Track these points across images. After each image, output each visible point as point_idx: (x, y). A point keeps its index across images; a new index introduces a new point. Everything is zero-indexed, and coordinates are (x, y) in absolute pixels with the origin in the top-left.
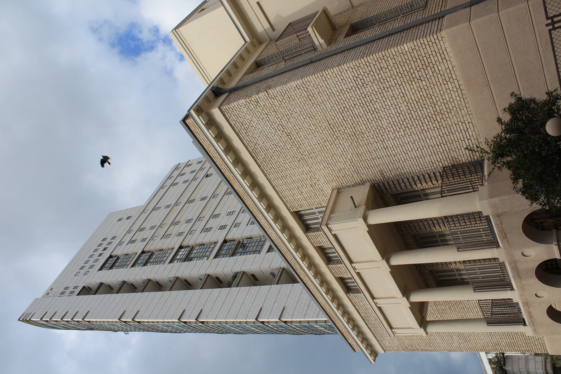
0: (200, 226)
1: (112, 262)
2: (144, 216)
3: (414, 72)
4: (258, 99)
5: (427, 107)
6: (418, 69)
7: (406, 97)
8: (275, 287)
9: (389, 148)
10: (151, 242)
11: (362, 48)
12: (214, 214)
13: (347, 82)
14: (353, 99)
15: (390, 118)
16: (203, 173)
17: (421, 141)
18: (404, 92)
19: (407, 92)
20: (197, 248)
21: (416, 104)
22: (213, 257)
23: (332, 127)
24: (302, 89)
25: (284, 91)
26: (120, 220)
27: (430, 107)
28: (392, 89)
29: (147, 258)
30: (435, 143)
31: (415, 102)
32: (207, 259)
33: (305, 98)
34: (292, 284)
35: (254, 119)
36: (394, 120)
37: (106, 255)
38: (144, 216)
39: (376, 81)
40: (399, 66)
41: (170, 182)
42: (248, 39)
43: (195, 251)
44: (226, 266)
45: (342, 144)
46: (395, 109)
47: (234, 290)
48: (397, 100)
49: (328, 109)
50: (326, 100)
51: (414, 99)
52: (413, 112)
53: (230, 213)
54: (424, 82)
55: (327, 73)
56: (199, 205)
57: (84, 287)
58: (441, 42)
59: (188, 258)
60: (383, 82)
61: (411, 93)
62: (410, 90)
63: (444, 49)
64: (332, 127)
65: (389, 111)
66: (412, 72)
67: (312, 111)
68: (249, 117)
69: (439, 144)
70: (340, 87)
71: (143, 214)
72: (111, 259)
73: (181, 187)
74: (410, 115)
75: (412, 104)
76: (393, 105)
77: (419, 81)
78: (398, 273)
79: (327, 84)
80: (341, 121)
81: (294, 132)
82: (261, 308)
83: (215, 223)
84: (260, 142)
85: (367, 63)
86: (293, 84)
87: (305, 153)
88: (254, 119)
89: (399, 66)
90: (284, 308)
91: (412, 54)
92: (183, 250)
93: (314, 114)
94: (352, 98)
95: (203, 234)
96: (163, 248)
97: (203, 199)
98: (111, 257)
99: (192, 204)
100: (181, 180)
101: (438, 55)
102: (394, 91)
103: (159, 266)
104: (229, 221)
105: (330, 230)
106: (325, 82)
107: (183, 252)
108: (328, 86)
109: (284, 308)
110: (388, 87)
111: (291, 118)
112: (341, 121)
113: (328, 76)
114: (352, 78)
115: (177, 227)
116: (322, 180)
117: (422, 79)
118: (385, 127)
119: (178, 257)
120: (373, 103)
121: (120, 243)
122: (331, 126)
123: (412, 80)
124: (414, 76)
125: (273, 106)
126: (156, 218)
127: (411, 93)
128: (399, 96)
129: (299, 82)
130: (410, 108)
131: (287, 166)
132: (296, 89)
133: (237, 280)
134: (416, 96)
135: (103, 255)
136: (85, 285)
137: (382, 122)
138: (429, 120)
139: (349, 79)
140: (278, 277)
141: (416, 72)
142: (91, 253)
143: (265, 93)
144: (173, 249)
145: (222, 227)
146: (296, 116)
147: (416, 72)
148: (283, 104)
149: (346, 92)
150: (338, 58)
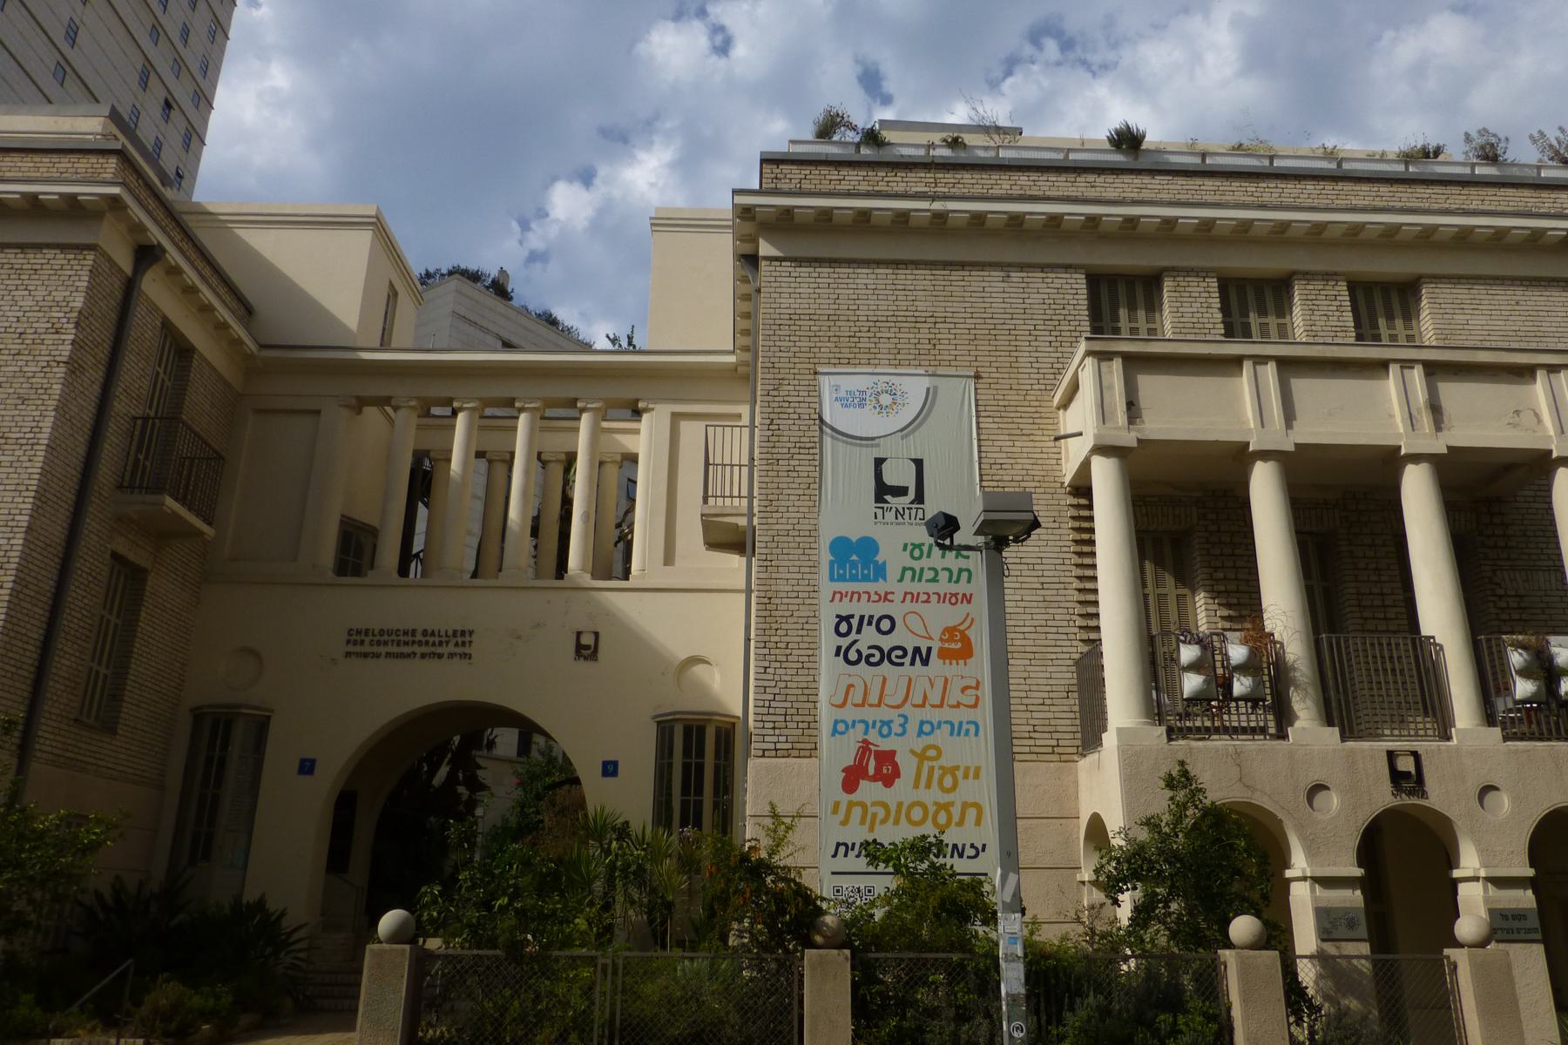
11: (49, 586)
68: (41, 292)
86: (47, 424)
129: (44, 438)
150: (56, 532)
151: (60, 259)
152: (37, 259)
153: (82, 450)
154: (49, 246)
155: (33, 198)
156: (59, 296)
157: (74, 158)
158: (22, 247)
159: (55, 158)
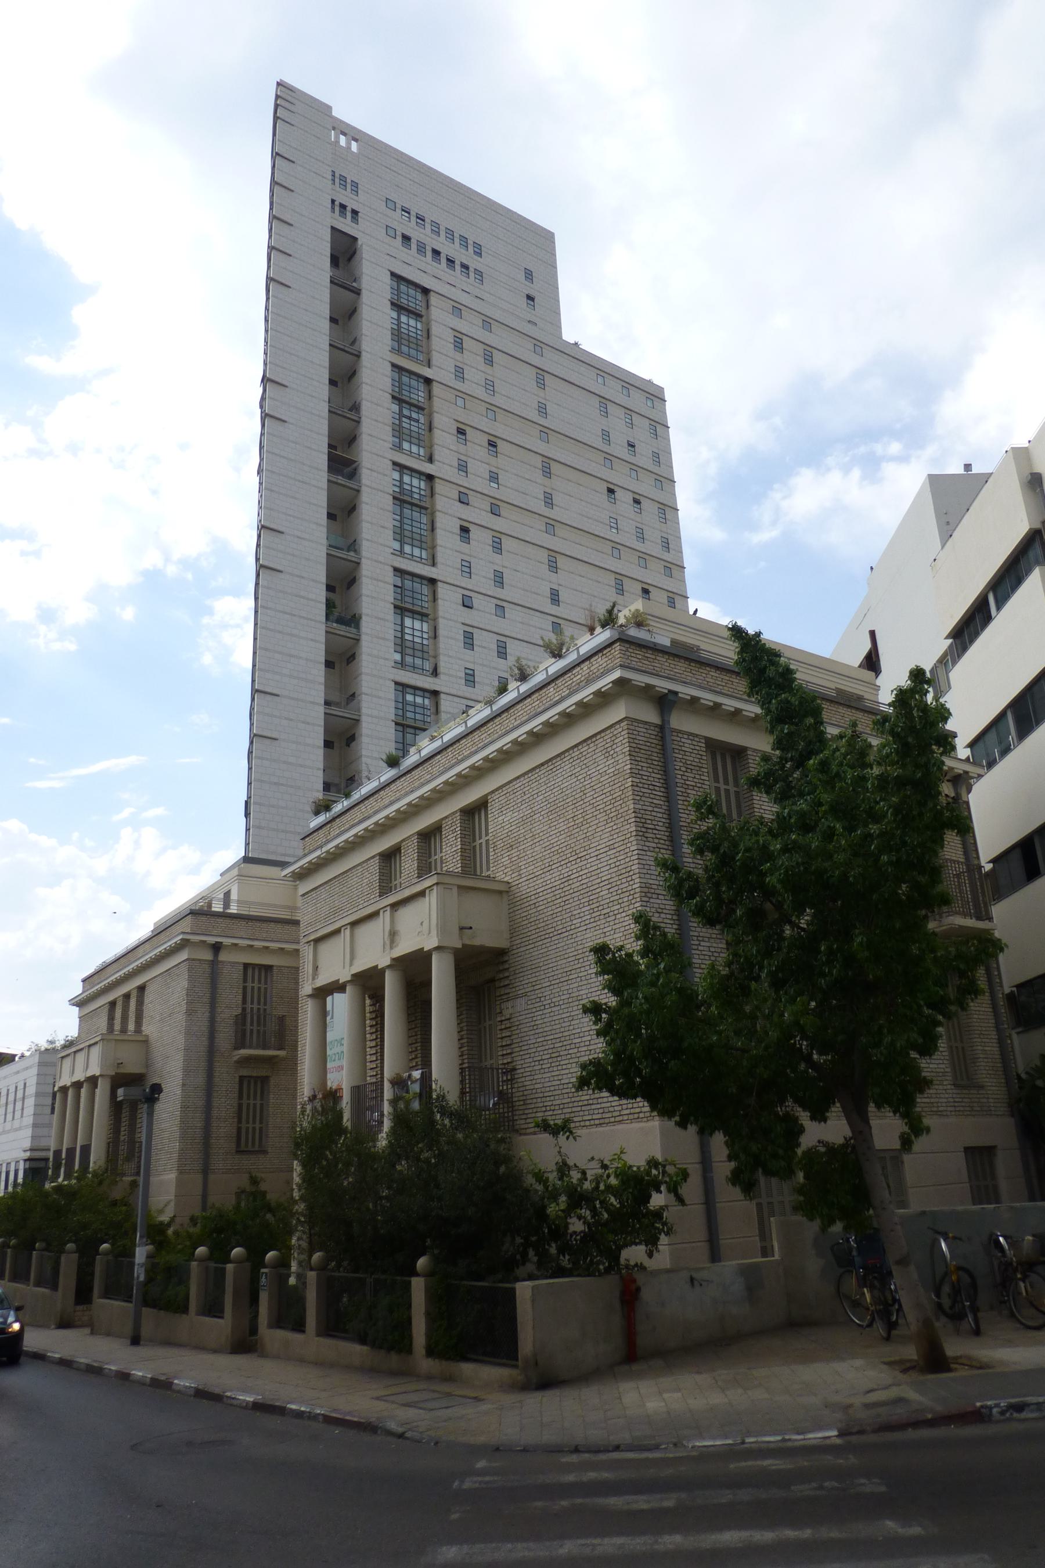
16: (618, 477)
22: (397, 565)
26: (529, 275)
29: (413, 395)
43: (416, 515)
44: (375, 597)
53: (499, 579)
57: (355, 239)
59: (401, 500)
92: (423, 485)
96: (437, 433)
98: (426, 291)
100: (616, 422)
119: (406, 479)
121: (458, 310)
126: (516, 391)
136: (360, 242)
140: (341, 714)
144: (431, 460)
150: (200, 1079)
153: (206, 1043)
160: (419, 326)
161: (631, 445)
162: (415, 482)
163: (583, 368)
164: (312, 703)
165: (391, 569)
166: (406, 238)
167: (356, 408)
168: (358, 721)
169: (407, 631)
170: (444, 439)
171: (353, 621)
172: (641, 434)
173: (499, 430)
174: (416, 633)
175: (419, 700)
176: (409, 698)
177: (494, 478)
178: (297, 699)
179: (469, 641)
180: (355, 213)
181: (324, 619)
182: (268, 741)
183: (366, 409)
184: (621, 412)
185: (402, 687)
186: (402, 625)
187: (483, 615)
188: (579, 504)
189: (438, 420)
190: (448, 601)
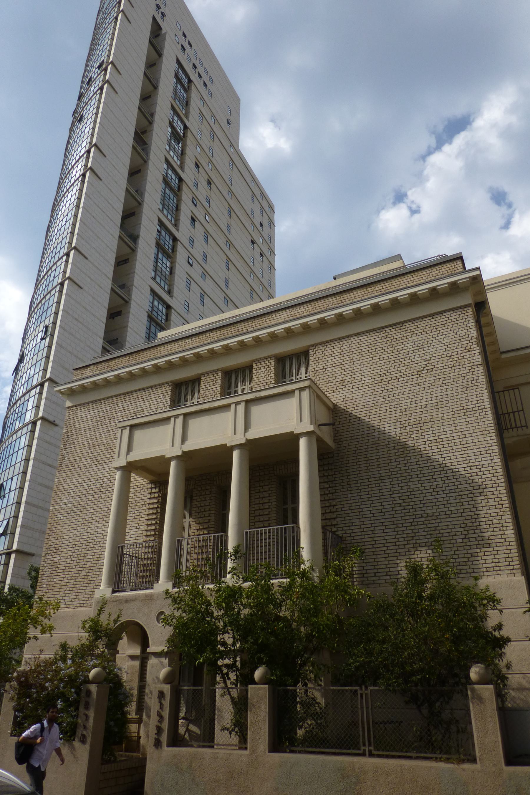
0: (199, 214)
1: (184, 82)
2: (226, 144)
3: (475, 533)
4: (473, 352)
5: (427, 537)
6: (478, 539)
7: (444, 517)
8: (108, 284)
9: (380, 482)
10: (195, 143)
12: (209, 237)
13: (477, 457)
14: (452, 458)
15: (420, 492)
17: (383, 521)
18: (451, 516)
19: (452, 519)
20: (175, 201)
21: (433, 525)
23: (420, 425)
24: (477, 405)
25: (478, 384)
27: (426, 540)
28: (458, 504)
30: (377, 535)
31: (436, 525)
32: (159, 209)
33: (464, 405)
34: (107, 306)
35: (447, 341)
36: (416, 496)
37: (194, 77)
38: (226, 144)
39: (471, 488)
40: (487, 519)
41: (257, 193)
42: (504, 356)
43: (172, 196)
45: (395, 430)
46: (430, 501)
47: (116, 231)
48: (443, 506)
49: (444, 427)
50: (457, 428)
51: (440, 524)
52: (423, 519)
54: (461, 541)
55: (492, 438)
56: (223, 221)
58: (509, 572)
60: (469, 496)
61: (449, 523)
62: (453, 523)
63: (499, 572)
64: (420, 425)
65: (430, 494)
66: (476, 531)
67: (445, 408)
68: (451, 334)
69: (375, 539)
70: (472, 448)
71: (229, 144)
72: (187, 80)
73: (248, 205)
74: (420, 516)
75: (433, 521)
76: (436, 500)
77: (463, 537)
78: (223, 453)
79: (478, 434)
80: (426, 436)
81: (420, 380)
82: (87, 258)
83: (198, 232)
84: (414, 338)
85: (496, 485)
87: (390, 385)
88: (447, 341)
89: (487, 519)
90: (81, 288)
91: (500, 536)
92: (177, 181)
93: (440, 409)
94: (454, 457)
95: (190, 215)
97: (229, 228)
98: (190, 81)
99: (226, 212)
101: (494, 565)
102: (455, 505)
103: (165, 142)
104: (197, 253)
105: (301, 389)
106: (482, 433)
107: (174, 180)
108: (475, 434)
109: (81, 288)
110: (462, 500)
111: (440, 383)
112: (426, 436)
113: (489, 438)
114: (481, 463)
115: (205, 183)
116: (349, 395)
117: (465, 540)
118: (409, 484)
119: (170, 172)
120: (443, 479)
122: (422, 425)
123: (466, 529)
124: (470, 532)
125: (461, 367)
126: (221, 161)
127: (449, 523)
128: (447, 509)
130: (429, 518)
131: (376, 359)
132: (478, 399)
133: (127, 240)
134: (444, 528)
135: (194, 72)
136: (163, 31)
137: (417, 483)
138: (409, 535)
139: (480, 460)
140: (119, 293)
141: (476, 535)
142: (200, 56)
143: (480, 363)
145: (192, 242)
146: (442, 388)
147: (476, 535)
148: (461, 378)
149: (463, 452)
151: (454, 316)
152: (443, 319)
154: (445, 311)
155: (434, 289)
156: (462, 333)
157: (438, 268)
158: (432, 315)
159: (429, 271)
160: (185, 95)
161: (261, 225)
162: (174, 177)
163: (247, 173)
164: (105, 275)
165: (157, 219)
166: (183, 48)
167: (152, 115)
168: (127, 302)
169: (159, 260)
170: (189, 163)
171: (135, 238)
172: (266, 223)
173: (213, 177)
174: (164, 265)
175: (160, 307)
176: (156, 303)
177: (208, 201)
178: (97, 268)
179: (189, 287)
180: (163, 15)
181: (119, 225)
182: (76, 287)
183: (157, 117)
184: (259, 206)
185: (153, 293)
186: (157, 255)
187: (196, 272)
188: (240, 240)
189: (188, 151)
190: (181, 256)
